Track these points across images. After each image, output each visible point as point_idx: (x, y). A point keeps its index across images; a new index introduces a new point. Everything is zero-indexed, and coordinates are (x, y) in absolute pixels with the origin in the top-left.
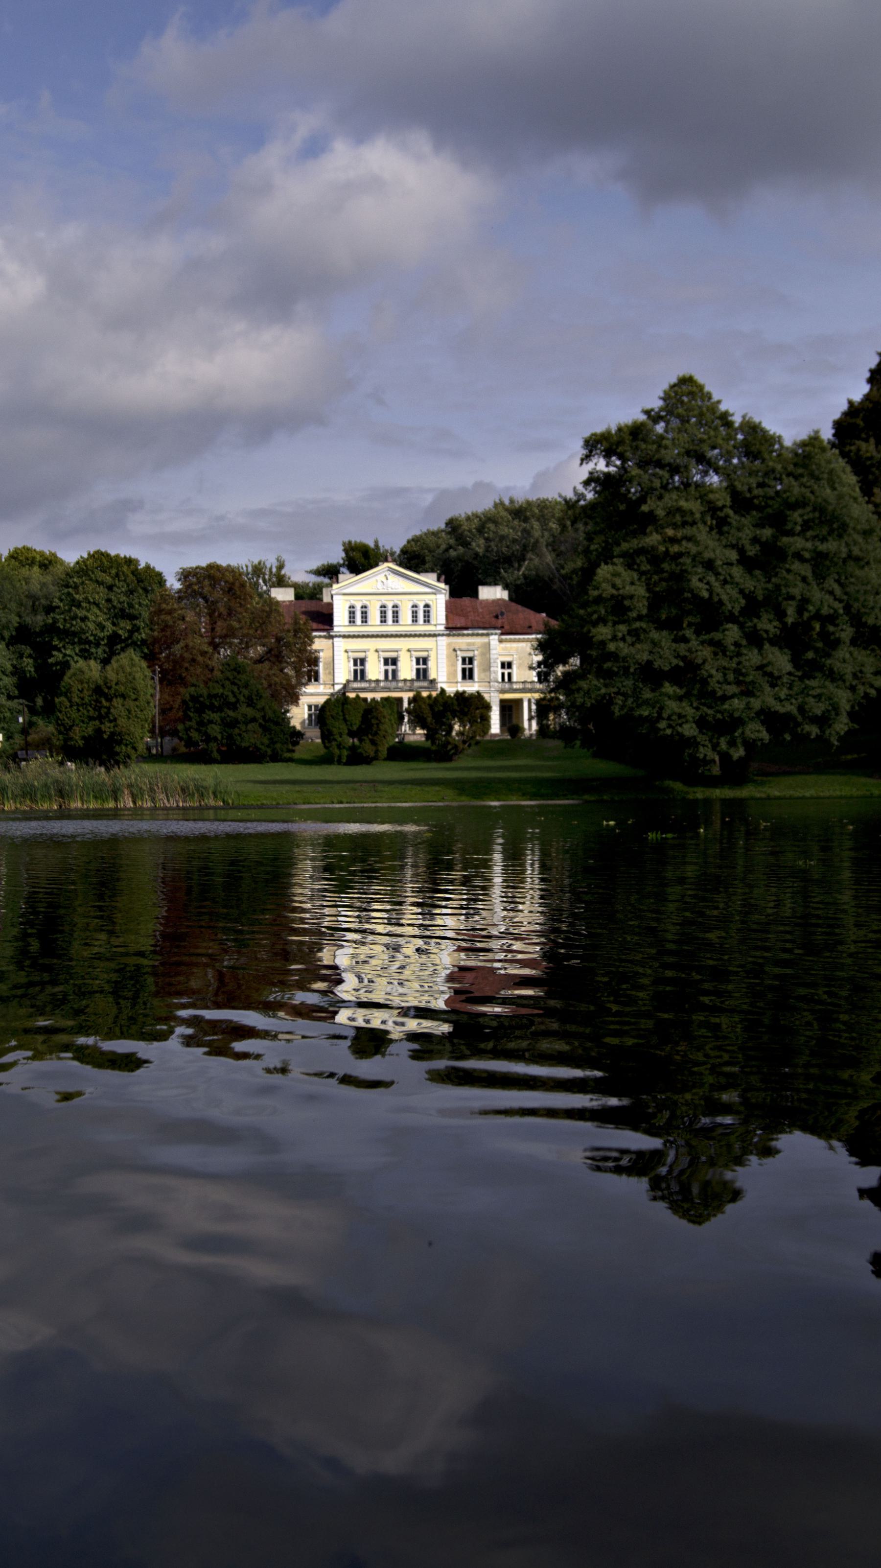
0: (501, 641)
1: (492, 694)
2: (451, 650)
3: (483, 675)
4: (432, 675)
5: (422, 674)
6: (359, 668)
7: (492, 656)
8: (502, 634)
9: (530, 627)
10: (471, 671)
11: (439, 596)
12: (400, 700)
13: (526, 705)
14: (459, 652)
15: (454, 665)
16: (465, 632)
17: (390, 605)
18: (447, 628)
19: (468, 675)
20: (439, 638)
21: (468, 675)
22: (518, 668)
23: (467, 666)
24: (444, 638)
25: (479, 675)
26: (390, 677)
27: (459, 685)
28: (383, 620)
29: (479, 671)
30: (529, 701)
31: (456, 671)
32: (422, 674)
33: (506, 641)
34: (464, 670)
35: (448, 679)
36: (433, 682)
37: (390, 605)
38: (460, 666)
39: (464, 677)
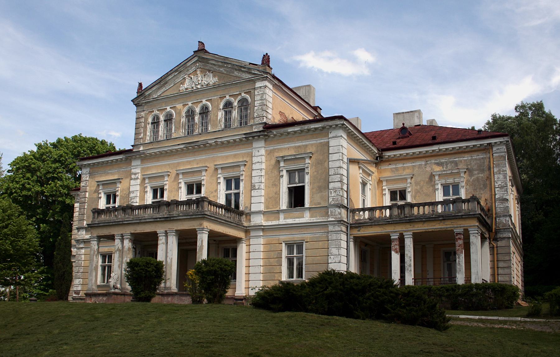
1: (331, 228)
2: (273, 162)
3: (317, 197)
7: (331, 164)
11: (258, 84)
13: (395, 245)
14: (282, 164)
15: (276, 184)
16: (290, 130)
19: (297, 197)
20: (255, 144)
22: (414, 197)
24: (262, 143)
25: (312, 197)
27: (282, 216)
29: (311, 189)
31: (278, 193)
35: (267, 207)
37: (198, 110)
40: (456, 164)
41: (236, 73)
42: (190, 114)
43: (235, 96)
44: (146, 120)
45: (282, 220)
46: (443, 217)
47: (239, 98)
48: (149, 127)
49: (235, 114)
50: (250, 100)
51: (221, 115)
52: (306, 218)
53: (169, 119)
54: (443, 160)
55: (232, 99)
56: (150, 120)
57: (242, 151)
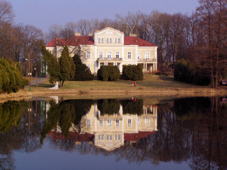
0: (138, 48)
4: (120, 57)
5: (117, 56)
6: (101, 54)
8: (139, 46)
9: (144, 44)
10: (130, 55)
12: (113, 63)
13: (144, 65)
15: (126, 54)
17: (109, 38)
18: (124, 44)
19: (129, 57)
21: (129, 57)
23: (129, 55)
26: (109, 58)
27: (127, 59)
28: (108, 43)
30: (145, 64)
32: (117, 56)
33: (139, 48)
34: (128, 56)
36: (121, 59)
37: (109, 38)
38: (127, 55)
39: (128, 58)
40: (149, 50)
41: (117, 33)
42: (108, 39)
43: (117, 37)
44: (97, 38)
45: (127, 60)
46: (151, 61)
47: (118, 38)
48: (98, 40)
49: (117, 41)
50: (120, 39)
51: (114, 40)
52: (132, 60)
53: (102, 39)
54: (146, 49)
55: (117, 38)
56: (98, 39)
57: (119, 48)
